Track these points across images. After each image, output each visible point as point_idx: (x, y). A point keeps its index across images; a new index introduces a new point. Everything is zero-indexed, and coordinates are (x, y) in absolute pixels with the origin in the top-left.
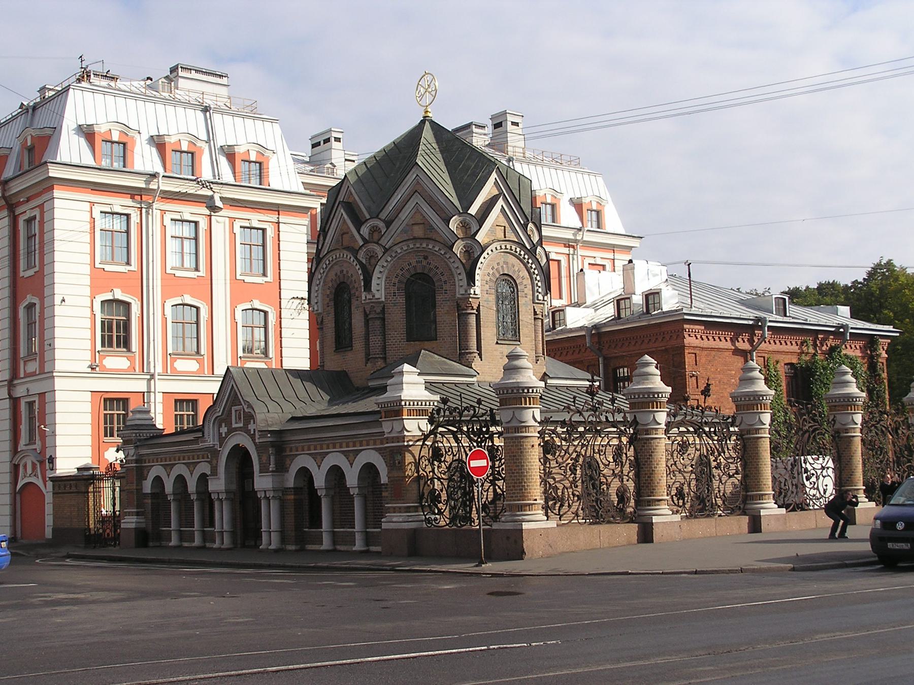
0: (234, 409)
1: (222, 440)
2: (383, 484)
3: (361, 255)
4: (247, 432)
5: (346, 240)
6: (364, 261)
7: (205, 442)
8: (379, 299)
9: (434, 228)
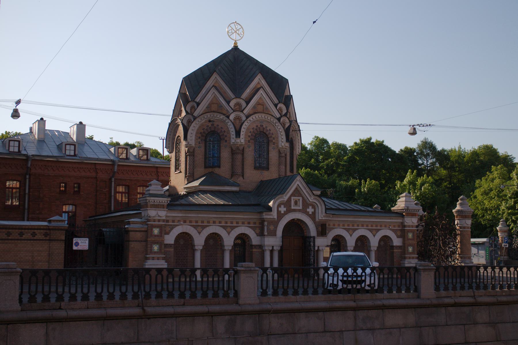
0: (292, 198)
1: (280, 216)
2: (395, 246)
4: (307, 213)
7: (271, 215)
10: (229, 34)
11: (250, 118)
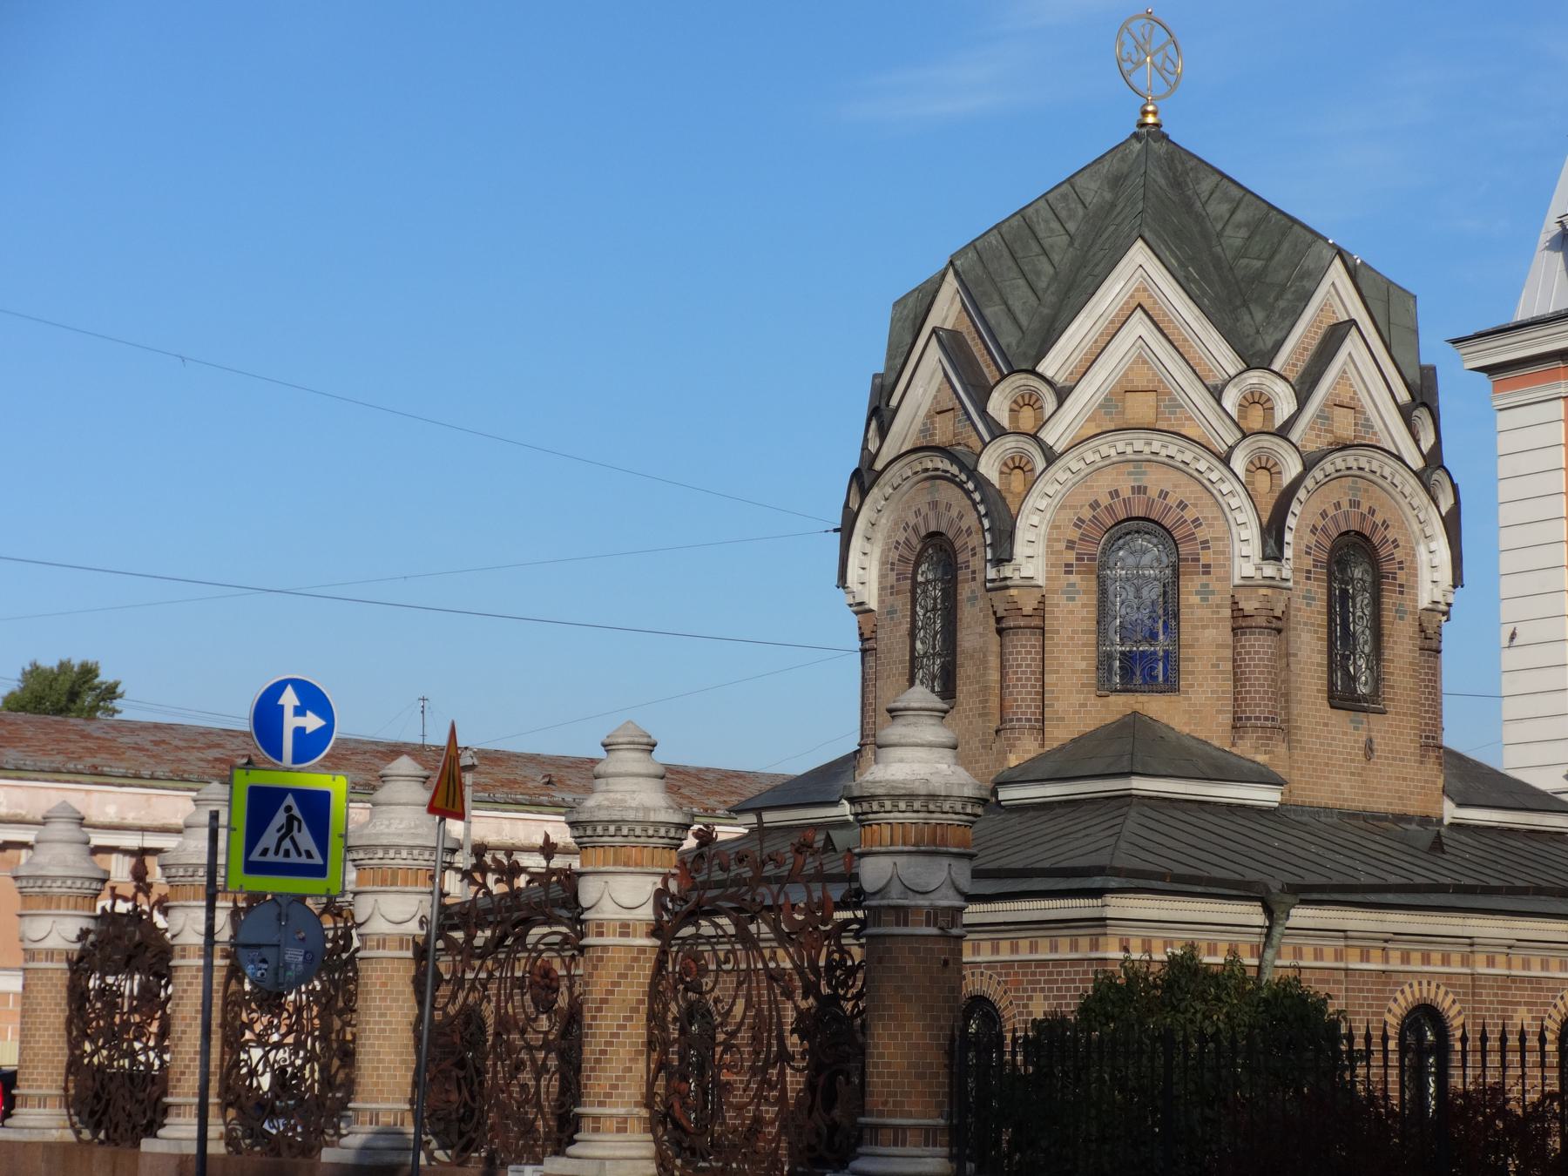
3: (1239, 463)
5: (1141, 408)
6: (1243, 478)
8: (1287, 580)
9: (1372, 427)
10: (1127, 66)
11: (1071, 461)
